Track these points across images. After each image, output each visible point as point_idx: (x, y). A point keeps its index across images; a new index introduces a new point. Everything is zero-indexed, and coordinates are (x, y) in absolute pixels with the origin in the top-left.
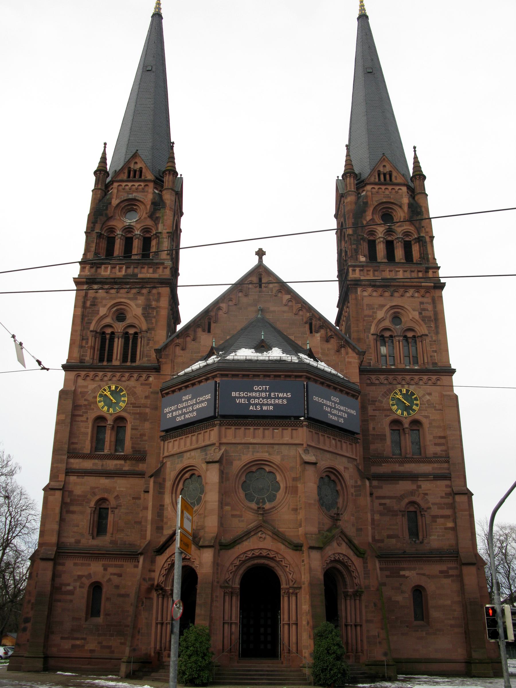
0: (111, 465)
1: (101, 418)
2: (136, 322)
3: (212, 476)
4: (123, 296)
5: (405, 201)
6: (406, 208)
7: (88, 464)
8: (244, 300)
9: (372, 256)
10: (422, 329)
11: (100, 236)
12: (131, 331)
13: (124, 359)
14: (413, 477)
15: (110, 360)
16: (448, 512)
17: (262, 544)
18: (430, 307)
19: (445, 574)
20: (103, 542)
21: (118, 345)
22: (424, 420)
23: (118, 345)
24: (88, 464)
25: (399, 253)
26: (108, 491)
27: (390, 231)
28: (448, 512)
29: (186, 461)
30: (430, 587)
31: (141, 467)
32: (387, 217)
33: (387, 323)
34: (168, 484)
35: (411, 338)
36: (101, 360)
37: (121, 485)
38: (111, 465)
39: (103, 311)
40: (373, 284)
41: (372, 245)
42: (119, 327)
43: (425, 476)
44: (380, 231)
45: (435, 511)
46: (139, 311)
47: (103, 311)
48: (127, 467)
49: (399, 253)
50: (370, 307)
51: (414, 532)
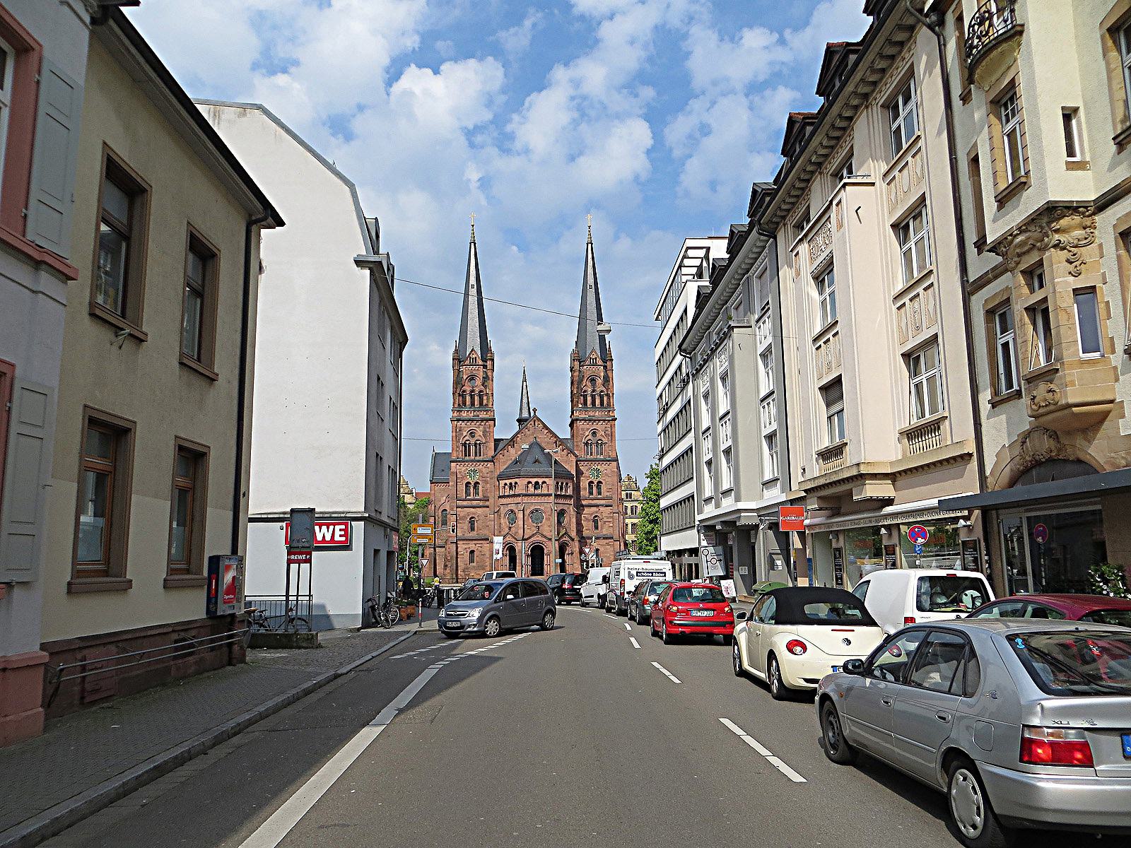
0: (475, 503)
1: (469, 483)
2: (480, 438)
3: (520, 515)
4: (473, 426)
5: (602, 374)
6: (602, 379)
7: (465, 503)
8: (528, 433)
9: (585, 403)
10: (605, 440)
11: (459, 395)
12: (478, 442)
13: (476, 455)
14: (597, 506)
15: (469, 456)
16: (611, 520)
17: (538, 538)
18: (609, 430)
19: (608, 544)
20: (473, 534)
21: (472, 448)
22: (603, 482)
23: (472, 448)
24: (465, 503)
25: (598, 402)
26: (474, 514)
27: (594, 391)
28: (611, 520)
29: (510, 507)
30: (602, 549)
31: (487, 503)
32: (593, 380)
33: (590, 437)
34: (502, 515)
35: (600, 444)
36: (466, 456)
37: (479, 511)
38: (475, 503)
39: (465, 434)
40: (585, 420)
41: (585, 397)
42: (473, 441)
43: (602, 505)
44: (590, 390)
45: (605, 519)
46: (481, 434)
47: (465, 434)
48: (481, 503)
49: (598, 402)
50: (583, 429)
51: (596, 528)
